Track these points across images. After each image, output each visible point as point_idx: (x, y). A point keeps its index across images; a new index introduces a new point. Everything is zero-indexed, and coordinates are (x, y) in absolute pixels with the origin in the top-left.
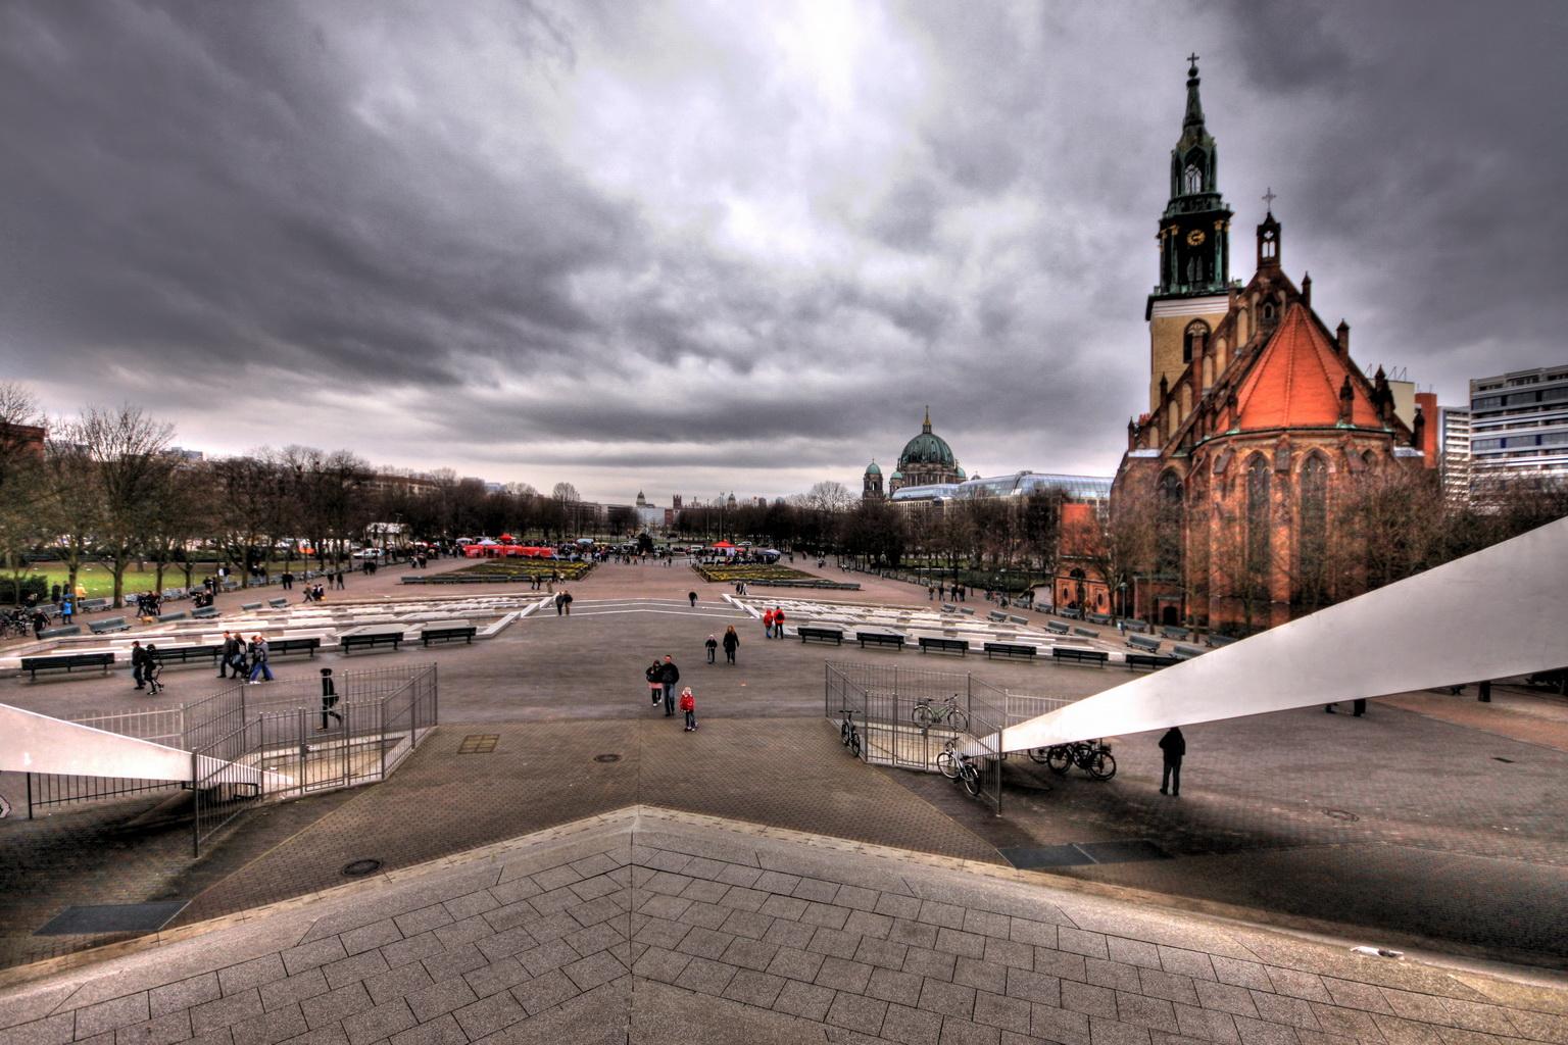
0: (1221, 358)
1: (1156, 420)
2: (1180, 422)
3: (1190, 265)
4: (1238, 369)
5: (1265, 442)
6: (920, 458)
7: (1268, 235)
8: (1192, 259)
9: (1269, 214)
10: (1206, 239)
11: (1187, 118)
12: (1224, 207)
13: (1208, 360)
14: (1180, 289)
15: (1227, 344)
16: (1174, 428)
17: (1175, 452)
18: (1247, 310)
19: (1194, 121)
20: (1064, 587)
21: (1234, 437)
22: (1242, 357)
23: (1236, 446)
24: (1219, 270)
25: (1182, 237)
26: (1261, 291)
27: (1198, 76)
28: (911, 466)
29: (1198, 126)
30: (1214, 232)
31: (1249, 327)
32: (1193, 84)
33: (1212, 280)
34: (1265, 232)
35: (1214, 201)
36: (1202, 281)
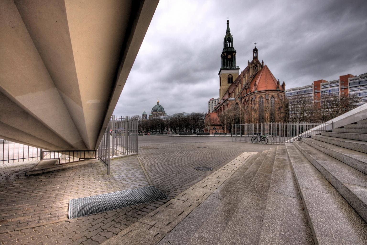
0: (246, 78)
1: (234, 91)
2: (238, 92)
4: (250, 80)
5: (263, 94)
6: (157, 110)
7: (255, 52)
8: (229, 61)
9: (255, 48)
11: (227, 31)
13: (244, 78)
14: (227, 67)
15: (248, 75)
16: (237, 94)
17: (238, 99)
18: (252, 68)
19: (228, 31)
20: (212, 132)
21: (256, 93)
23: (257, 95)
24: (234, 64)
25: (227, 56)
26: (254, 64)
27: (229, 22)
28: (154, 112)
29: (229, 33)
30: (233, 56)
31: (252, 71)
32: (228, 23)
33: (233, 66)
34: (255, 51)
35: (233, 49)
36: (231, 66)
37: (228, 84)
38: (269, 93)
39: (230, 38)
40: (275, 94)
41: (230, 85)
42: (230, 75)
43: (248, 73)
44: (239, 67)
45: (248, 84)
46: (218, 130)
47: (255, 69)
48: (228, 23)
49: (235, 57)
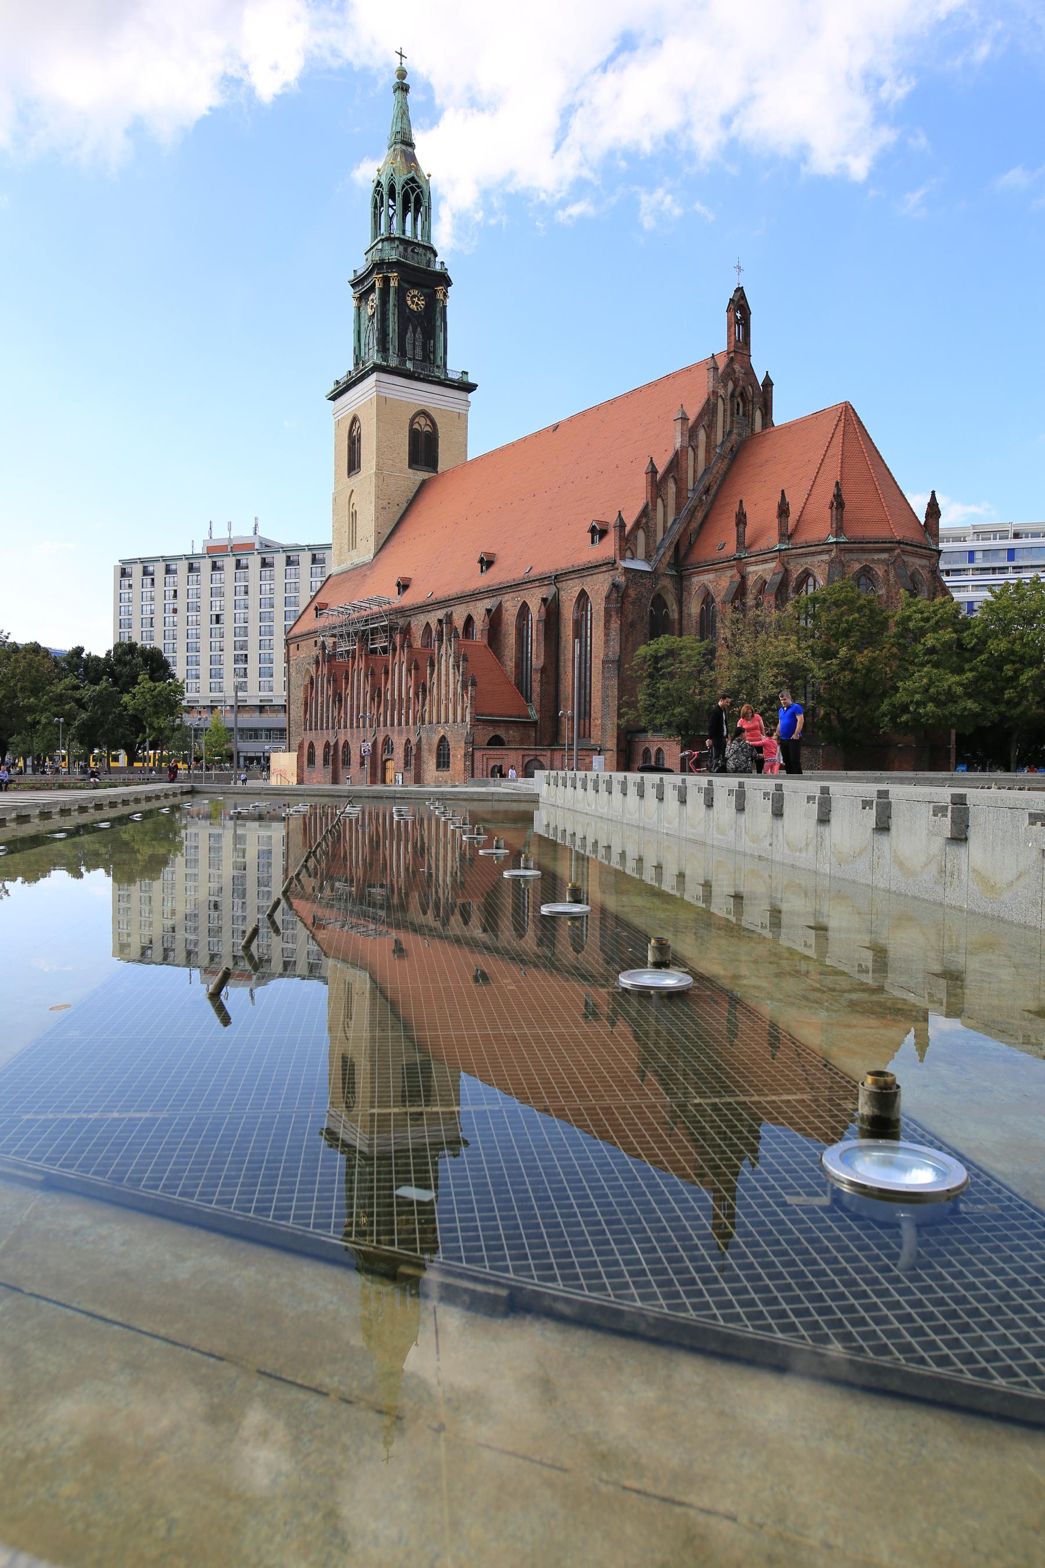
2: (665, 527)
3: (408, 336)
10: (426, 305)
12: (438, 267)
16: (660, 536)
22: (722, 457)
29: (410, 149)
39: (419, 187)
43: (710, 428)
45: (707, 491)
46: (549, 753)
47: (738, 413)
48: (403, 88)
49: (445, 307)
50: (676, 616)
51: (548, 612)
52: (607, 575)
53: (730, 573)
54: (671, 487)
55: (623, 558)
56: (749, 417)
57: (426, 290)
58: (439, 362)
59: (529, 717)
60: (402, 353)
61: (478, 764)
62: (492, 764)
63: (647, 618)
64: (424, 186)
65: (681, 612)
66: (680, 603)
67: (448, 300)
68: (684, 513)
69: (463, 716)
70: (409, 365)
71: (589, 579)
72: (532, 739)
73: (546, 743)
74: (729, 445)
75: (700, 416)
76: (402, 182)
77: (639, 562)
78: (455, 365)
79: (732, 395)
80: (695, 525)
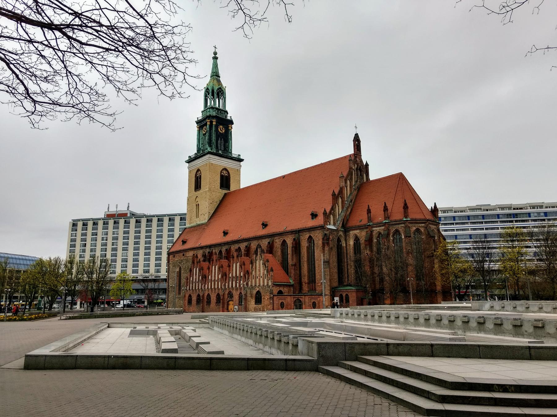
3: (219, 141)
5: (420, 225)
10: (225, 131)
12: (229, 118)
19: (215, 75)
22: (355, 190)
29: (219, 78)
32: (215, 58)
35: (227, 114)
37: (221, 190)
38: (430, 226)
39: (222, 91)
40: (435, 228)
41: (225, 191)
42: (225, 169)
43: (351, 180)
44: (242, 157)
46: (303, 297)
48: (215, 58)
50: (345, 245)
51: (296, 244)
52: (320, 231)
53: (365, 230)
54: (340, 200)
55: (327, 225)
56: (362, 175)
57: (225, 126)
58: (230, 151)
59: (290, 283)
60: (217, 147)
61: (276, 302)
62: (281, 301)
63: (336, 246)
64: (224, 91)
65: (346, 244)
66: (346, 240)
67: (232, 129)
68: (345, 209)
69: (268, 283)
70: (220, 152)
71: (312, 232)
72: (292, 291)
73: (297, 293)
74: (357, 185)
75: (348, 176)
76: (216, 89)
77: (332, 226)
78: (235, 151)
79: (357, 169)
80: (348, 213)
